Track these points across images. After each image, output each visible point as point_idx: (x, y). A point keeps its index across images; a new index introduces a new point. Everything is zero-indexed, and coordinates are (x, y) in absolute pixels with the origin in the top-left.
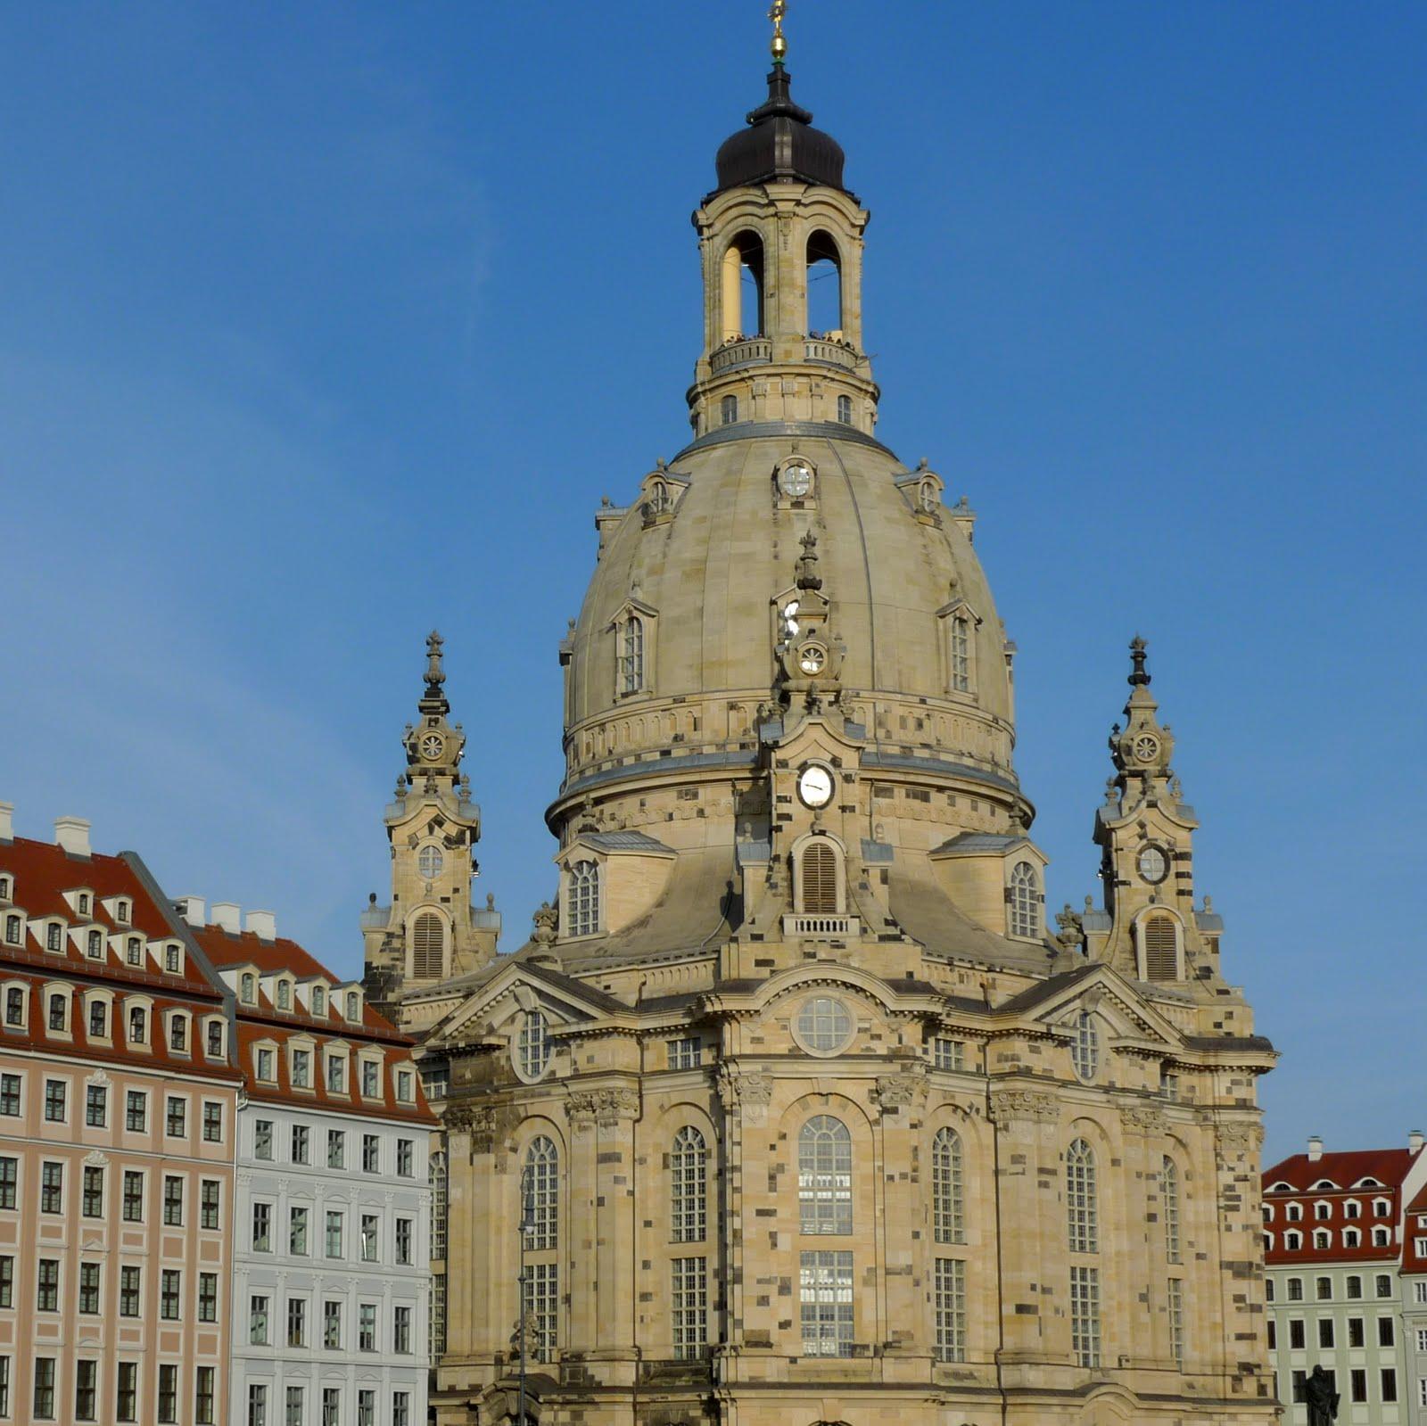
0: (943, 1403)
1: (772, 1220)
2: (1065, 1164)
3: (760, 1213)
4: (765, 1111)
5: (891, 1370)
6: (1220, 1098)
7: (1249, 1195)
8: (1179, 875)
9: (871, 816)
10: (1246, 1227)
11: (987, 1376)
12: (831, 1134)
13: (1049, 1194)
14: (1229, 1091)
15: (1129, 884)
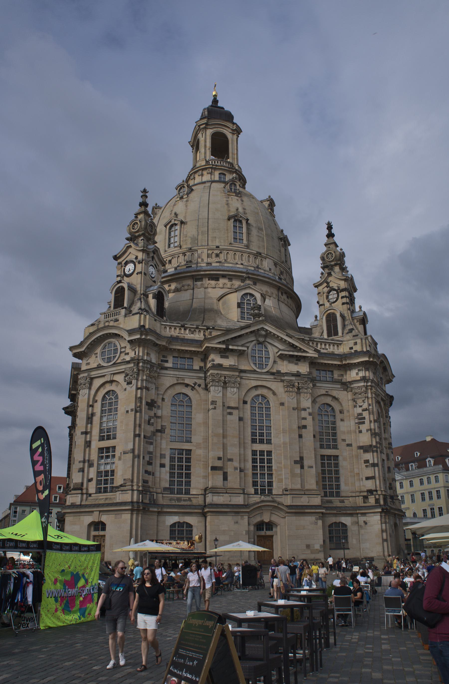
0: (159, 513)
1: (88, 436)
2: (248, 406)
3: (82, 433)
4: (87, 391)
5: (120, 497)
6: (354, 377)
7: (368, 416)
8: (342, 297)
9: (193, 289)
10: (367, 430)
11: (200, 501)
12: (113, 397)
13: (234, 418)
14: (357, 374)
15: (324, 305)
